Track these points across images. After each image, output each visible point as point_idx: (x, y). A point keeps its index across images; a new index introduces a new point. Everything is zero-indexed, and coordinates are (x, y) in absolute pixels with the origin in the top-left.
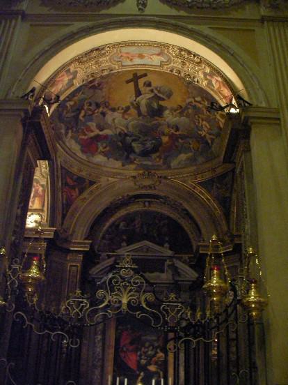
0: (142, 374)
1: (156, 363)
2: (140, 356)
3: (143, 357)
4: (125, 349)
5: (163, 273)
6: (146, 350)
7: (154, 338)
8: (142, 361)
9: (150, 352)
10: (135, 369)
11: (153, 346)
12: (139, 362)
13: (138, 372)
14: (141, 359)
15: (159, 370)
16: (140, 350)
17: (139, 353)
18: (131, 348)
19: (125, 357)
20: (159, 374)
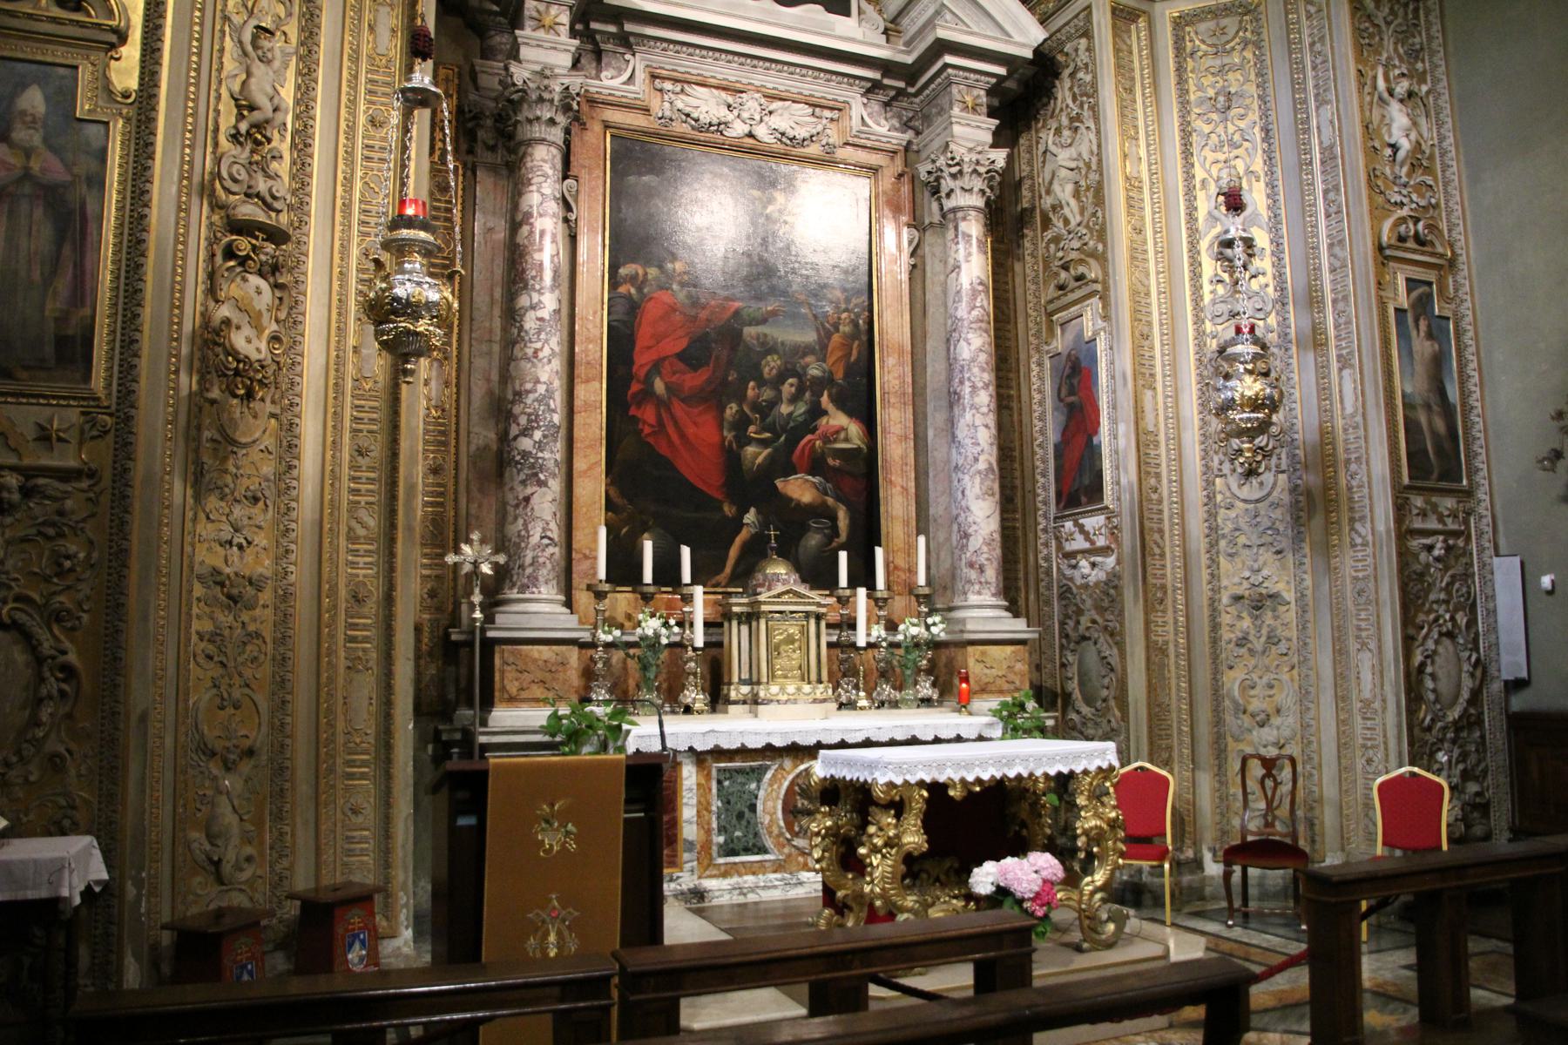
0: (750, 517)
1: (816, 466)
2: (741, 423)
3: (752, 428)
4: (659, 386)
5: (847, 13)
6: (767, 394)
7: (809, 337)
8: (750, 450)
9: (785, 409)
10: (719, 496)
11: (800, 376)
12: (732, 458)
13: (728, 510)
14: (746, 441)
15: (830, 501)
16: (741, 397)
17: (731, 410)
18: (694, 380)
19: (661, 424)
20: (834, 519)
